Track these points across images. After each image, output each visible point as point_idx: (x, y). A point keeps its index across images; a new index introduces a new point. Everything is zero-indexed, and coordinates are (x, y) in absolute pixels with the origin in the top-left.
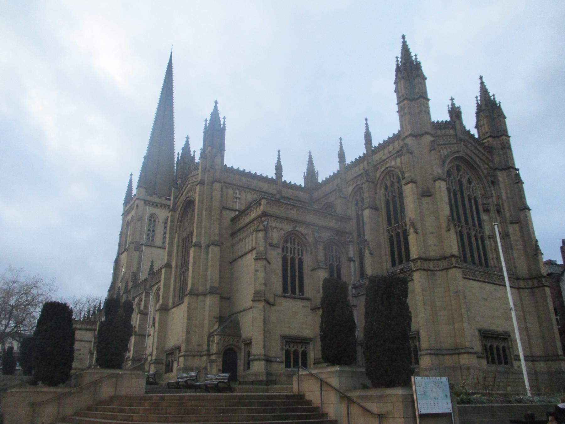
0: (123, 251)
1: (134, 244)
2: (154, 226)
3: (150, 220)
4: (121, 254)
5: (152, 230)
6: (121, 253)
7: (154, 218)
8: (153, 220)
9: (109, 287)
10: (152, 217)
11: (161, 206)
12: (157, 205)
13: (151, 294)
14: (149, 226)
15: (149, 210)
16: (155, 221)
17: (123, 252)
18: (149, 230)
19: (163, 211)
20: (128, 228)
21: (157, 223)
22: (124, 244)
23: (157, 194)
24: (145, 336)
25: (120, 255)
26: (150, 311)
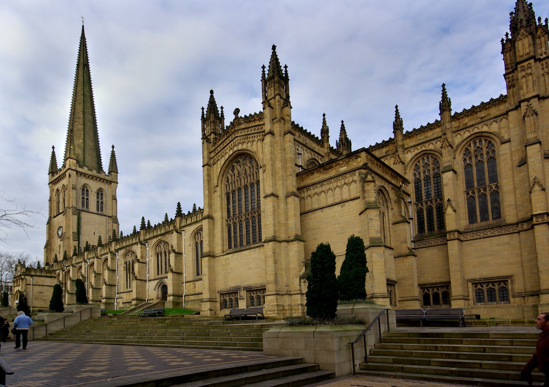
0: (55, 215)
1: (71, 209)
2: (87, 195)
3: (83, 190)
4: (54, 217)
5: (85, 198)
6: (53, 217)
7: (86, 188)
8: (85, 189)
9: (45, 244)
10: (84, 187)
11: (92, 178)
12: (89, 177)
13: (147, 246)
14: (83, 194)
15: (83, 181)
16: (87, 191)
17: (57, 215)
18: (83, 198)
19: (95, 182)
20: (59, 195)
21: (90, 192)
22: (55, 209)
23: (87, 167)
24: (146, 281)
25: (52, 219)
26: (148, 260)
